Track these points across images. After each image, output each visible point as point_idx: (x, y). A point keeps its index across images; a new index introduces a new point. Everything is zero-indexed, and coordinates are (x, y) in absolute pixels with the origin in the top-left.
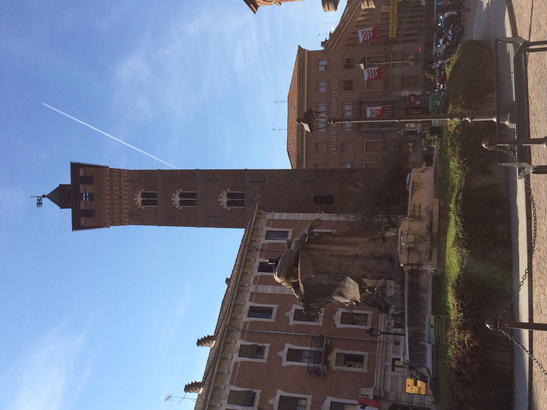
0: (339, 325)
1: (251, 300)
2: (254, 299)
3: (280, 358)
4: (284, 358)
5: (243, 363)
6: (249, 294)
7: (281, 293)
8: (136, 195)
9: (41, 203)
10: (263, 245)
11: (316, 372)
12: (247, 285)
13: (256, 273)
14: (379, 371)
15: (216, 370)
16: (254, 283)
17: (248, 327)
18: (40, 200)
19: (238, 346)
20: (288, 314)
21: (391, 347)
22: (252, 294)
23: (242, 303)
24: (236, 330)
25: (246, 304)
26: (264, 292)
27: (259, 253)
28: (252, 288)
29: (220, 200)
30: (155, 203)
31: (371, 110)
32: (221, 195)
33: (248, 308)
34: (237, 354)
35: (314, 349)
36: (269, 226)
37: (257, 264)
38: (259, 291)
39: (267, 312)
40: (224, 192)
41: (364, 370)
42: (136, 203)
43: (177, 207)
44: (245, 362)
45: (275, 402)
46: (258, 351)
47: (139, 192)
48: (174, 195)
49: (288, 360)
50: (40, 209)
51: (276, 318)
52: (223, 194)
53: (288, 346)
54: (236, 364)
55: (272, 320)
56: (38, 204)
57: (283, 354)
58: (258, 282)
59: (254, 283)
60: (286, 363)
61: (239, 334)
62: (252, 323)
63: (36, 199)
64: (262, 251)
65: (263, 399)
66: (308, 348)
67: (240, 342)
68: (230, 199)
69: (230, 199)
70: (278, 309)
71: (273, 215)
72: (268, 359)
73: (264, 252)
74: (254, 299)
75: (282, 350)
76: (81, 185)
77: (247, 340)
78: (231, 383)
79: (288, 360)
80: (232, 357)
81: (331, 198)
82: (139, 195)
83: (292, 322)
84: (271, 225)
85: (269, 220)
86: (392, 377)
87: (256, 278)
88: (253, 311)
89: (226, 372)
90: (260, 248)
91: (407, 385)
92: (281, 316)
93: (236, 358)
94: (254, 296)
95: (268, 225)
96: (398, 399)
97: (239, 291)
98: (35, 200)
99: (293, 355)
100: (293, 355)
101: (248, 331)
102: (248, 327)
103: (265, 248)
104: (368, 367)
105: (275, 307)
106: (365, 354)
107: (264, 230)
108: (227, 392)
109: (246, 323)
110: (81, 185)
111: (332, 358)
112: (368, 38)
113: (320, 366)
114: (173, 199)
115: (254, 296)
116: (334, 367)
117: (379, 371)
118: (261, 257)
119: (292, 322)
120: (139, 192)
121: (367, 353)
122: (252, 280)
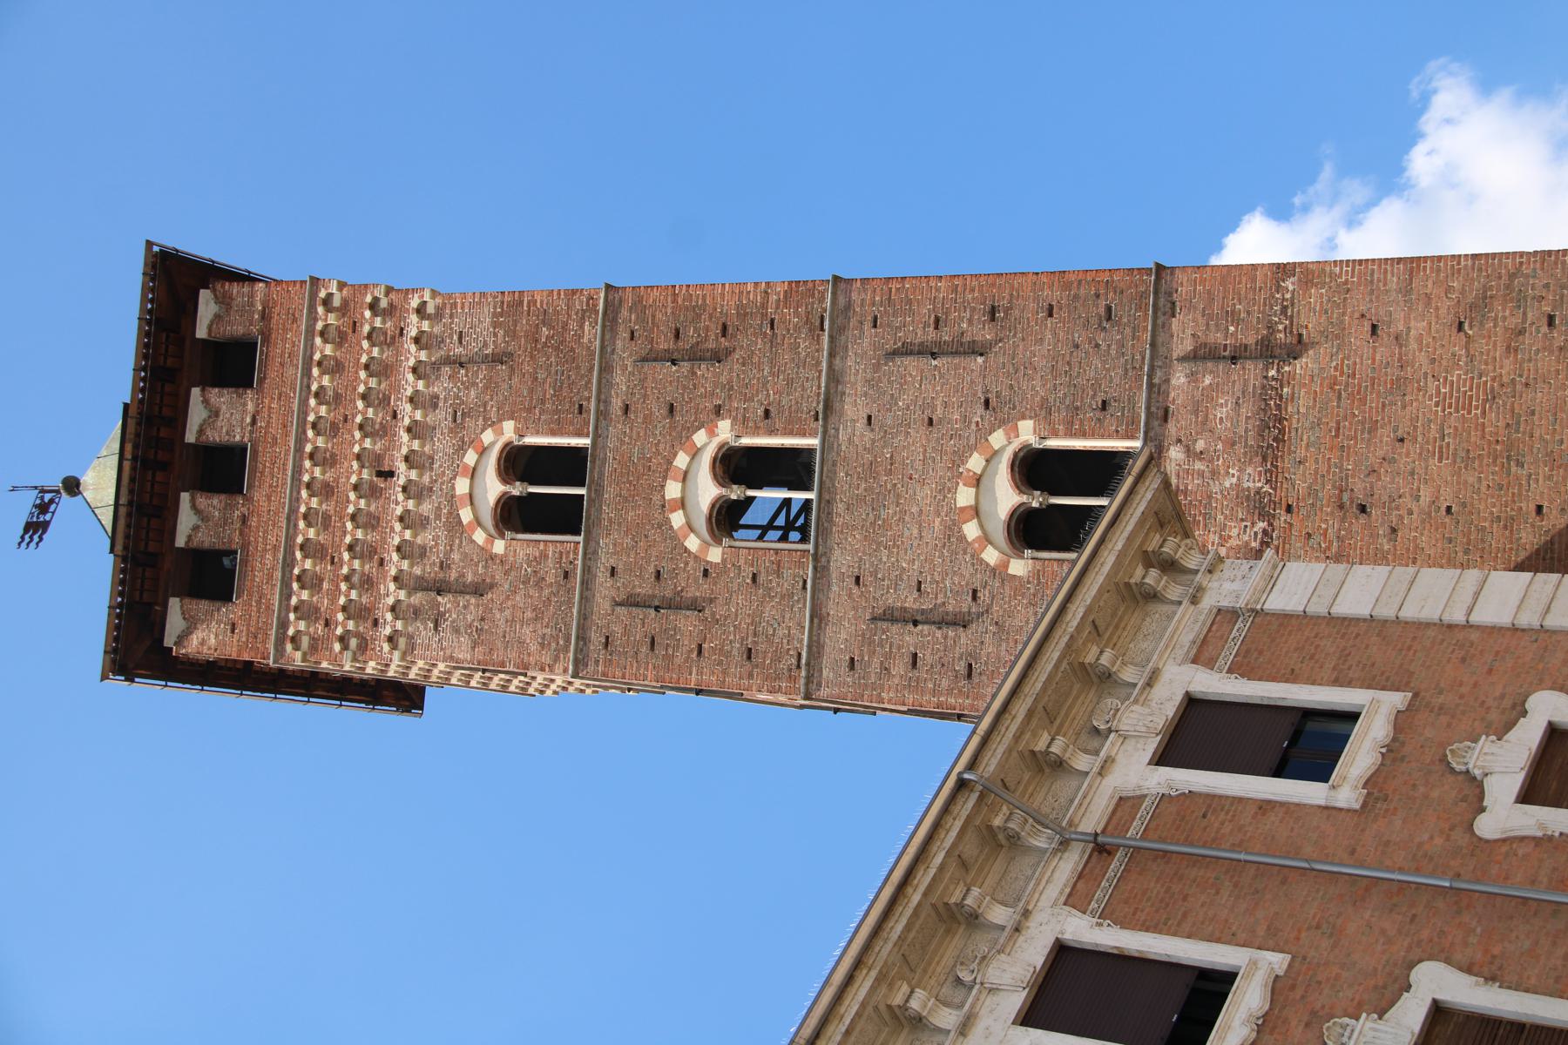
8: (470, 458)
10: (1126, 804)
18: (43, 508)
27: (1067, 867)
32: (975, 463)
36: (1210, 664)
40: (997, 439)
42: (466, 515)
43: (693, 543)
48: (681, 460)
63: (31, 497)
64: (1101, 849)
68: (1036, 500)
69: (1036, 500)
71: (1271, 581)
73: (1116, 864)
84: (1229, 654)
85: (1228, 615)
90: (1092, 821)
95: (1202, 655)
103: (1136, 828)
107: (1159, 691)
114: (673, 490)
118: (1076, 899)
120: (488, 437)
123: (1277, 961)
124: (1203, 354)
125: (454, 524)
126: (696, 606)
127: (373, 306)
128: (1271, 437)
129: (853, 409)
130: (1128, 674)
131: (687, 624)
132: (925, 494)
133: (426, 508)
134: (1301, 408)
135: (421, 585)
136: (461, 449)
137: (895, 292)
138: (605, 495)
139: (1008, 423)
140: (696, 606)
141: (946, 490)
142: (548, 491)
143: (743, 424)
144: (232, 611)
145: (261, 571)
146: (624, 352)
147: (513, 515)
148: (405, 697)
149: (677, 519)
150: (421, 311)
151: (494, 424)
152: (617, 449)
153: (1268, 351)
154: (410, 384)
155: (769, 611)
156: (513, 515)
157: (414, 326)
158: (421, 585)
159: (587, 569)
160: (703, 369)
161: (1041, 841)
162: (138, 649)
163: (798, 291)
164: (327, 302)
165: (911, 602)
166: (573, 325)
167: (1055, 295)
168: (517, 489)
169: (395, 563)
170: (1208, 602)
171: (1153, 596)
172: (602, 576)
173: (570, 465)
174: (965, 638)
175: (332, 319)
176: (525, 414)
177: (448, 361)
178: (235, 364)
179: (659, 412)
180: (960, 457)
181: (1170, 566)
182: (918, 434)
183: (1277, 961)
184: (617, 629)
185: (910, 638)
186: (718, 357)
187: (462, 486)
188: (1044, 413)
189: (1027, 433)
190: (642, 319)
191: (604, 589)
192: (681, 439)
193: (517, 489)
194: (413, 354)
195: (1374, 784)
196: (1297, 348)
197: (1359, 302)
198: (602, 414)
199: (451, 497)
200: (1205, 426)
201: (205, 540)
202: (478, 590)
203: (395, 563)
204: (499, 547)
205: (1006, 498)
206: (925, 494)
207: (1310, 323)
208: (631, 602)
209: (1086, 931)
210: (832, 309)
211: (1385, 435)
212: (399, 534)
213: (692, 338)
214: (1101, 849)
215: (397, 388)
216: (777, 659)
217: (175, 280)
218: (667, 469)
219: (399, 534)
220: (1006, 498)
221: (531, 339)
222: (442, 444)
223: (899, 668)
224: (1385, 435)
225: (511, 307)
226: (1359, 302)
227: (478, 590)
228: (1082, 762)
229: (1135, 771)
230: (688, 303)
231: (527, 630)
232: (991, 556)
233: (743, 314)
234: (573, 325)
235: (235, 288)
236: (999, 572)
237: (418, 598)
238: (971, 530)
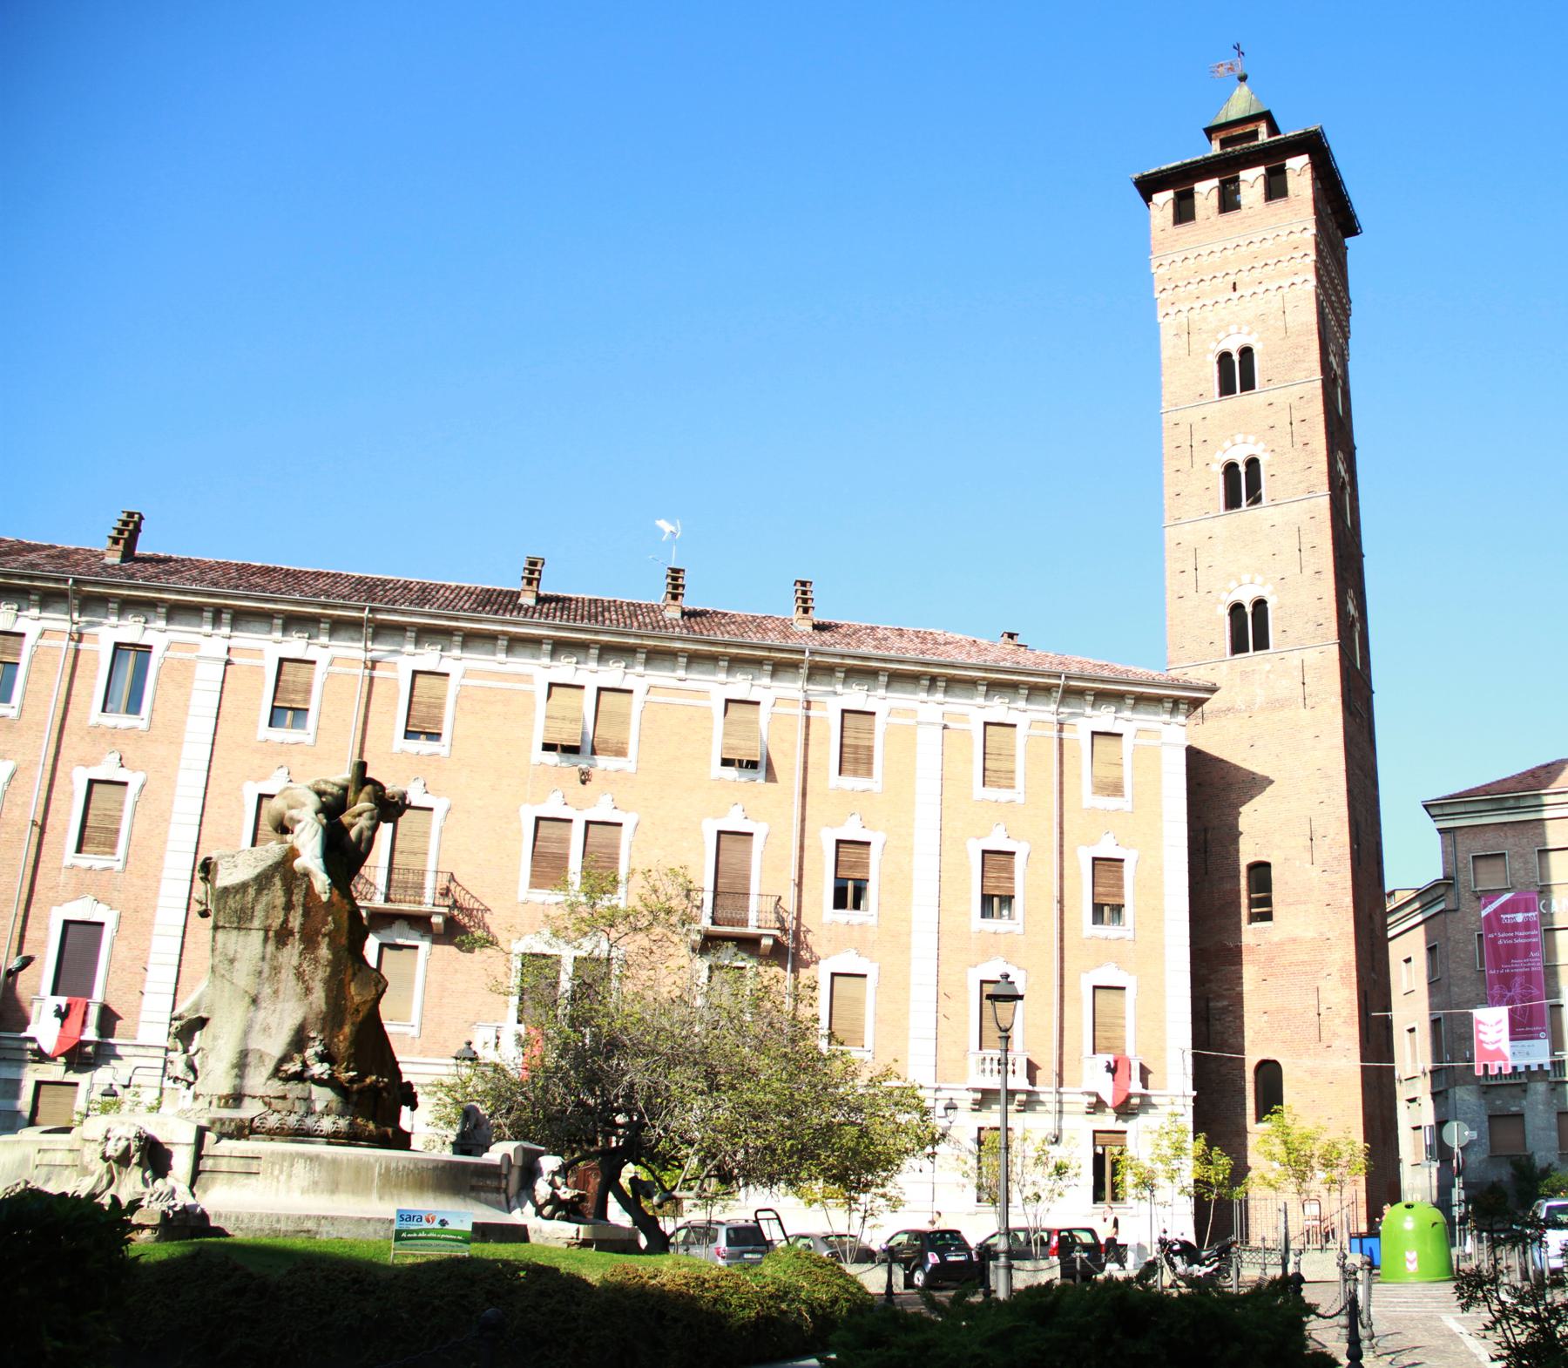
15: (678, 645)
29: (1245, 578)
30: (1226, 388)
38: (922, 733)
42: (1221, 336)
47: (1255, 335)
48: (1251, 439)
52: (1262, 586)
68: (1249, 609)
81: (1267, 917)
114: (1239, 438)
123: (1020, 799)
128: (1277, 704)
136: (1249, 323)
149: (1227, 444)
166: (1305, 365)
174: (1190, 591)
184: (1181, 428)
185: (1190, 569)
187: (1233, 329)
191: (1194, 415)
195: (1093, 808)
201: (1199, 200)
234: (1305, 365)
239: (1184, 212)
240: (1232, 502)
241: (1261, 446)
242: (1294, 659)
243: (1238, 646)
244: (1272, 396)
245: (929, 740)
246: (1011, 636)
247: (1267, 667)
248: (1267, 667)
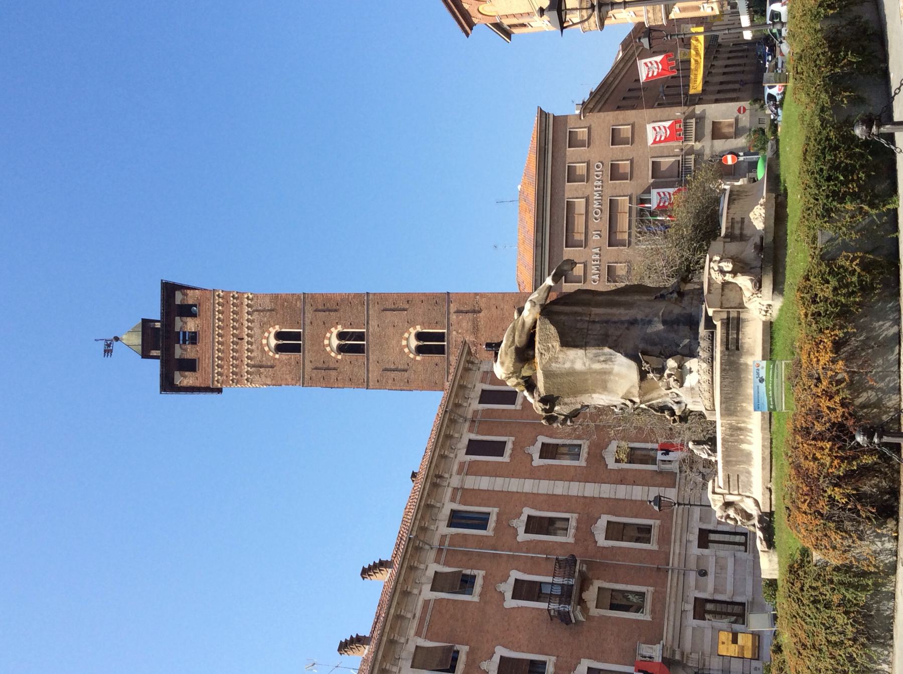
0: (602, 541)
1: (453, 500)
2: (458, 497)
3: (502, 594)
4: (509, 594)
5: (438, 601)
6: (449, 492)
7: (505, 489)
8: (266, 334)
9: (111, 351)
10: (476, 412)
11: (564, 618)
12: (446, 475)
13: (462, 456)
14: (671, 618)
16: (459, 473)
17: (447, 543)
18: (109, 345)
19: (430, 573)
20: (514, 523)
21: (692, 577)
22: (455, 490)
23: (438, 505)
24: (427, 547)
25: (445, 506)
26: (476, 487)
27: (467, 425)
28: (455, 481)
29: (404, 343)
30: (296, 349)
31: (659, 193)
32: (406, 335)
33: (448, 513)
34: (429, 586)
35: (558, 580)
37: (465, 442)
38: (467, 486)
39: (481, 521)
41: (645, 616)
42: (266, 349)
43: (333, 354)
44: (442, 600)
45: (492, 666)
46: (465, 583)
47: (271, 329)
48: (328, 335)
49: (514, 597)
50: (108, 359)
51: (495, 529)
53: (515, 575)
54: (427, 603)
55: (489, 532)
56: (105, 351)
57: (507, 588)
58: (465, 470)
59: (459, 473)
60: (510, 603)
61: (432, 555)
62: (453, 536)
63: (103, 343)
64: (473, 421)
65: (472, 663)
66: (549, 579)
67: (433, 568)
68: (421, 343)
69: (421, 343)
70: (498, 514)
72: (481, 595)
74: (458, 497)
75: (505, 581)
76: (177, 319)
77: (446, 564)
78: (418, 634)
79: (514, 597)
80: (421, 591)
82: (272, 335)
83: (522, 536)
86: (694, 628)
87: (462, 465)
88: (456, 519)
89: (409, 615)
90: (470, 416)
91: (720, 641)
92: (504, 526)
93: (427, 593)
94: (459, 494)
96: (704, 665)
97: (435, 485)
98: (101, 346)
99: (523, 590)
100: (523, 590)
101: (448, 550)
102: (447, 543)
104: (653, 612)
105: (494, 511)
106: (648, 590)
107: (476, 389)
108: (411, 647)
109: (444, 537)
110: (177, 319)
111: (591, 595)
112: (655, 74)
113: (569, 608)
114: (326, 342)
115: (459, 494)
116: (594, 611)
117: (671, 618)
118: (471, 430)
119: (522, 536)
121: (651, 589)
122: (456, 467)
123: (513, 439)
124: (458, 312)
125: (263, 351)
126: (334, 369)
127: (233, 297)
129: (373, 323)
130: (469, 386)
131: (333, 373)
132: (394, 342)
133: (254, 347)
134: (482, 324)
135: (254, 366)
136: (263, 332)
137: (383, 297)
138: (306, 343)
139: (414, 327)
140: (334, 369)
141: (399, 342)
142: (289, 343)
143: (344, 326)
144: (197, 374)
145: (204, 364)
146: (308, 307)
147: (279, 349)
148: (219, 391)
149: (328, 349)
150: (248, 298)
151: (273, 326)
152: (308, 332)
153: (474, 312)
154: (246, 316)
155: (356, 369)
156: (279, 349)
157: (246, 302)
158: (254, 366)
159: (304, 361)
160: (332, 313)
161: (461, 420)
162: (168, 385)
163: (357, 295)
164: (218, 296)
165: (392, 367)
167: (423, 298)
168: (280, 342)
169: (246, 361)
170: (481, 370)
171: (471, 369)
172: (307, 362)
173: (297, 336)
174: (406, 374)
175: (221, 300)
176: (282, 325)
177: (257, 311)
178: (187, 311)
179: (321, 324)
180: (403, 333)
181: (472, 363)
182: (391, 329)
183: (513, 439)
185: (393, 375)
186: (336, 311)
187: (264, 341)
188: (423, 324)
189: (419, 329)
190: (314, 302)
192: (328, 330)
193: (280, 342)
194: (246, 309)
196: (480, 312)
197: (493, 302)
198: (304, 324)
199: (262, 344)
200: (461, 327)
202: (272, 367)
203: (246, 361)
204: (277, 356)
205: (414, 343)
206: (394, 342)
207: (483, 305)
208: (316, 368)
209: (474, 437)
210: (365, 300)
211: (500, 329)
212: (246, 354)
213: (329, 307)
214: (473, 421)
215: (242, 317)
216: (358, 380)
217: (169, 290)
218: (324, 337)
219: (246, 354)
220: (414, 343)
221: (280, 306)
222: (257, 331)
223: (390, 381)
224: (500, 329)
225: (275, 297)
226: (493, 302)
227: (272, 367)
228: (465, 404)
229: (475, 405)
230: (327, 298)
231: (288, 376)
232: (412, 356)
233: (342, 300)
235: (188, 291)
236: (414, 359)
237: (253, 369)
238: (406, 350)
239: (190, 365)
240: (359, 349)
241: (333, 329)
242: (453, 317)
243: (440, 350)
244: (308, 321)
245: (471, 482)
246: (414, 475)
247: (454, 333)
248: (454, 333)
